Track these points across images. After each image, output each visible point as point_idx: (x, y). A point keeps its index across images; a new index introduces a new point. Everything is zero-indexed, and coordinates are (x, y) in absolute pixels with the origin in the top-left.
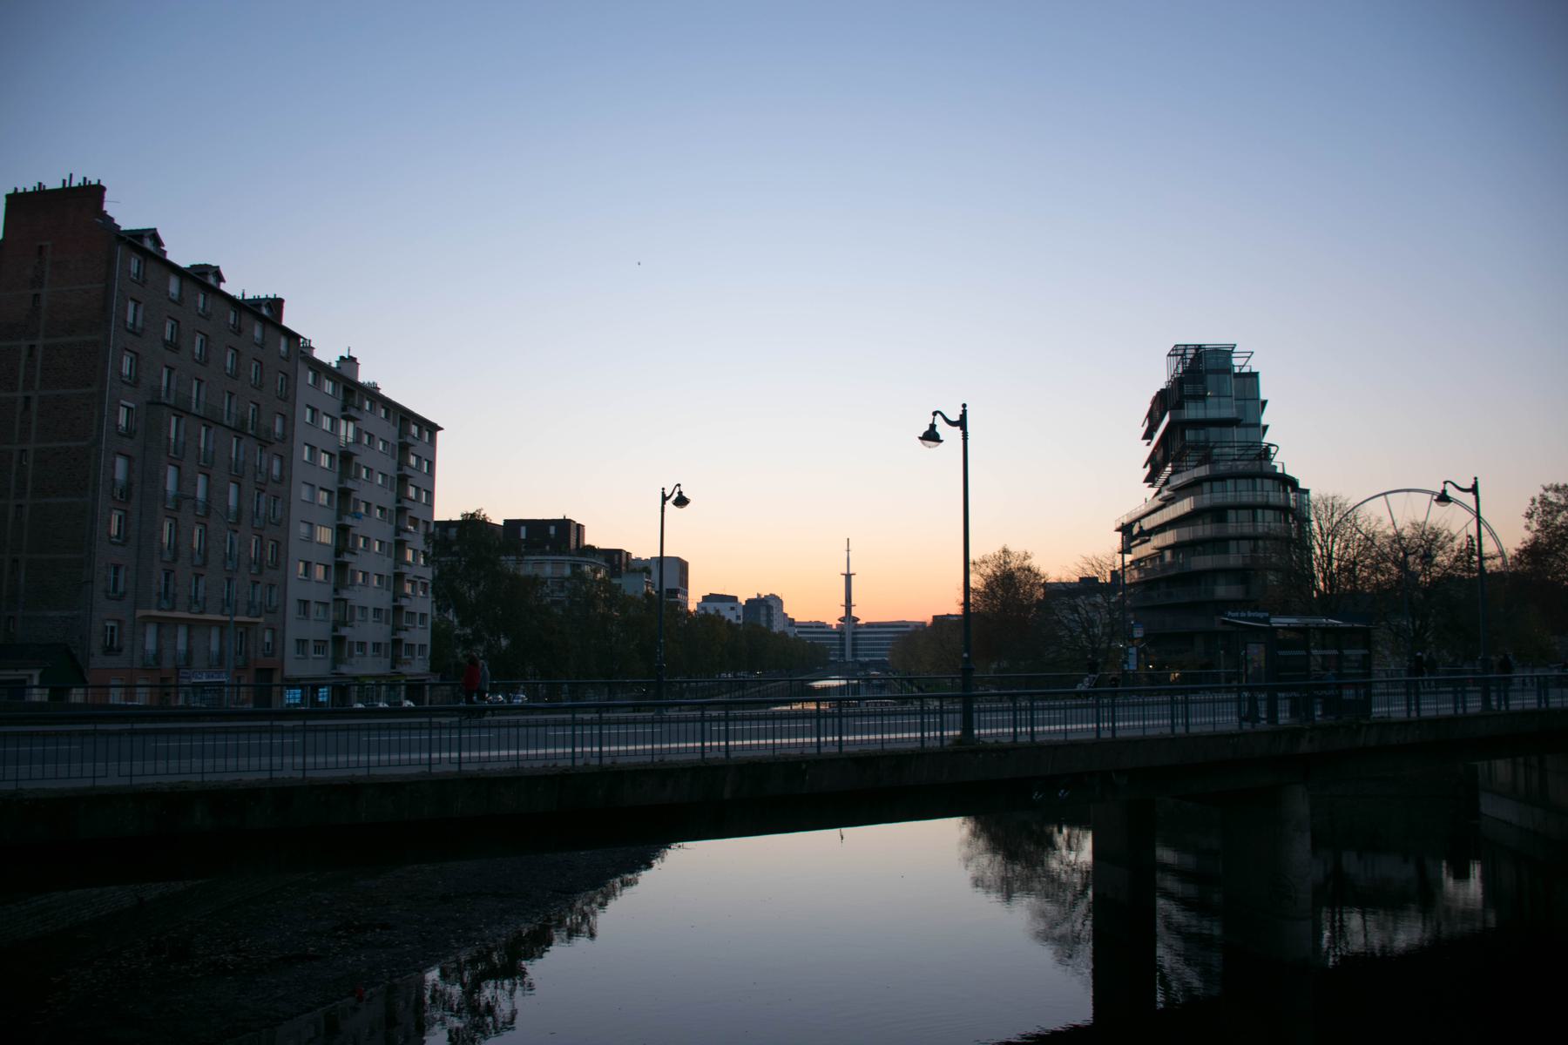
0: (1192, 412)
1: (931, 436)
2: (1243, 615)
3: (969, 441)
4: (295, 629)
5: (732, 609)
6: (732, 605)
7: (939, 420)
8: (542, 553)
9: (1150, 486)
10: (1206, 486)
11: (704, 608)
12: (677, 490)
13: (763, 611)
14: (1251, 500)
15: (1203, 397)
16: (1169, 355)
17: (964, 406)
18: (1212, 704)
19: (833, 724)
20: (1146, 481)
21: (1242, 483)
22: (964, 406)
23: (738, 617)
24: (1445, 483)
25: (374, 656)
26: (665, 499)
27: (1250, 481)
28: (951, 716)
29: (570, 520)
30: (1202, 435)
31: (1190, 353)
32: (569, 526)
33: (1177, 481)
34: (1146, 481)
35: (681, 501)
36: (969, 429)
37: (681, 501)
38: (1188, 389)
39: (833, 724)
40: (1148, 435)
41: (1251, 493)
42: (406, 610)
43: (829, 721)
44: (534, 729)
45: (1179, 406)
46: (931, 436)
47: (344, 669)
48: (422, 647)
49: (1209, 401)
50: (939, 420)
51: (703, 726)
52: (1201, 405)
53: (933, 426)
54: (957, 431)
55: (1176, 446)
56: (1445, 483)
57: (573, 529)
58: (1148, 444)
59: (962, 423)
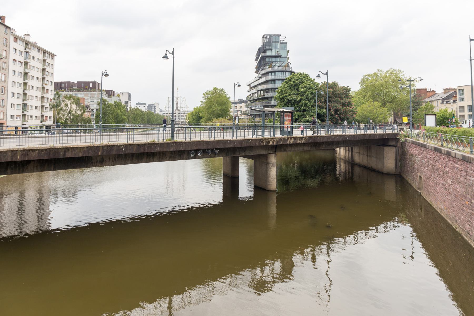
0: (268, 53)
1: (166, 57)
2: (256, 107)
3: (174, 58)
4: (10, 112)
5: (144, 107)
6: (144, 106)
7: (168, 52)
8: (88, 91)
9: (257, 74)
10: (270, 74)
11: (136, 107)
12: (106, 72)
13: (153, 108)
14: (282, 77)
15: (271, 49)
16: (262, 37)
17: (174, 49)
18: (200, 134)
19: (100, 140)
20: (255, 73)
21: (280, 73)
22: (174, 49)
23: (146, 109)
24: (319, 72)
25: (35, 120)
26: (102, 74)
27: (282, 72)
28: (167, 135)
29: (96, 82)
30: (270, 60)
31: (268, 37)
32: (96, 84)
33: (263, 72)
34: (255, 73)
35: (107, 75)
36: (175, 55)
37: (107, 75)
38: (267, 47)
39: (100, 140)
40: (256, 60)
41: (282, 76)
42: (45, 106)
43: (131, 136)
44: (51, 138)
45: (265, 52)
46: (166, 57)
47: (25, 123)
48: (50, 117)
49: (273, 50)
50: (168, 52)
51: (127, 136)
52: (270, 51)
53: (166, 54)
54: (172, 55)
55: (264, 62)
56: (319, 72)
57: (97, 84)
58: (256, 62)
59: (173, 53)
